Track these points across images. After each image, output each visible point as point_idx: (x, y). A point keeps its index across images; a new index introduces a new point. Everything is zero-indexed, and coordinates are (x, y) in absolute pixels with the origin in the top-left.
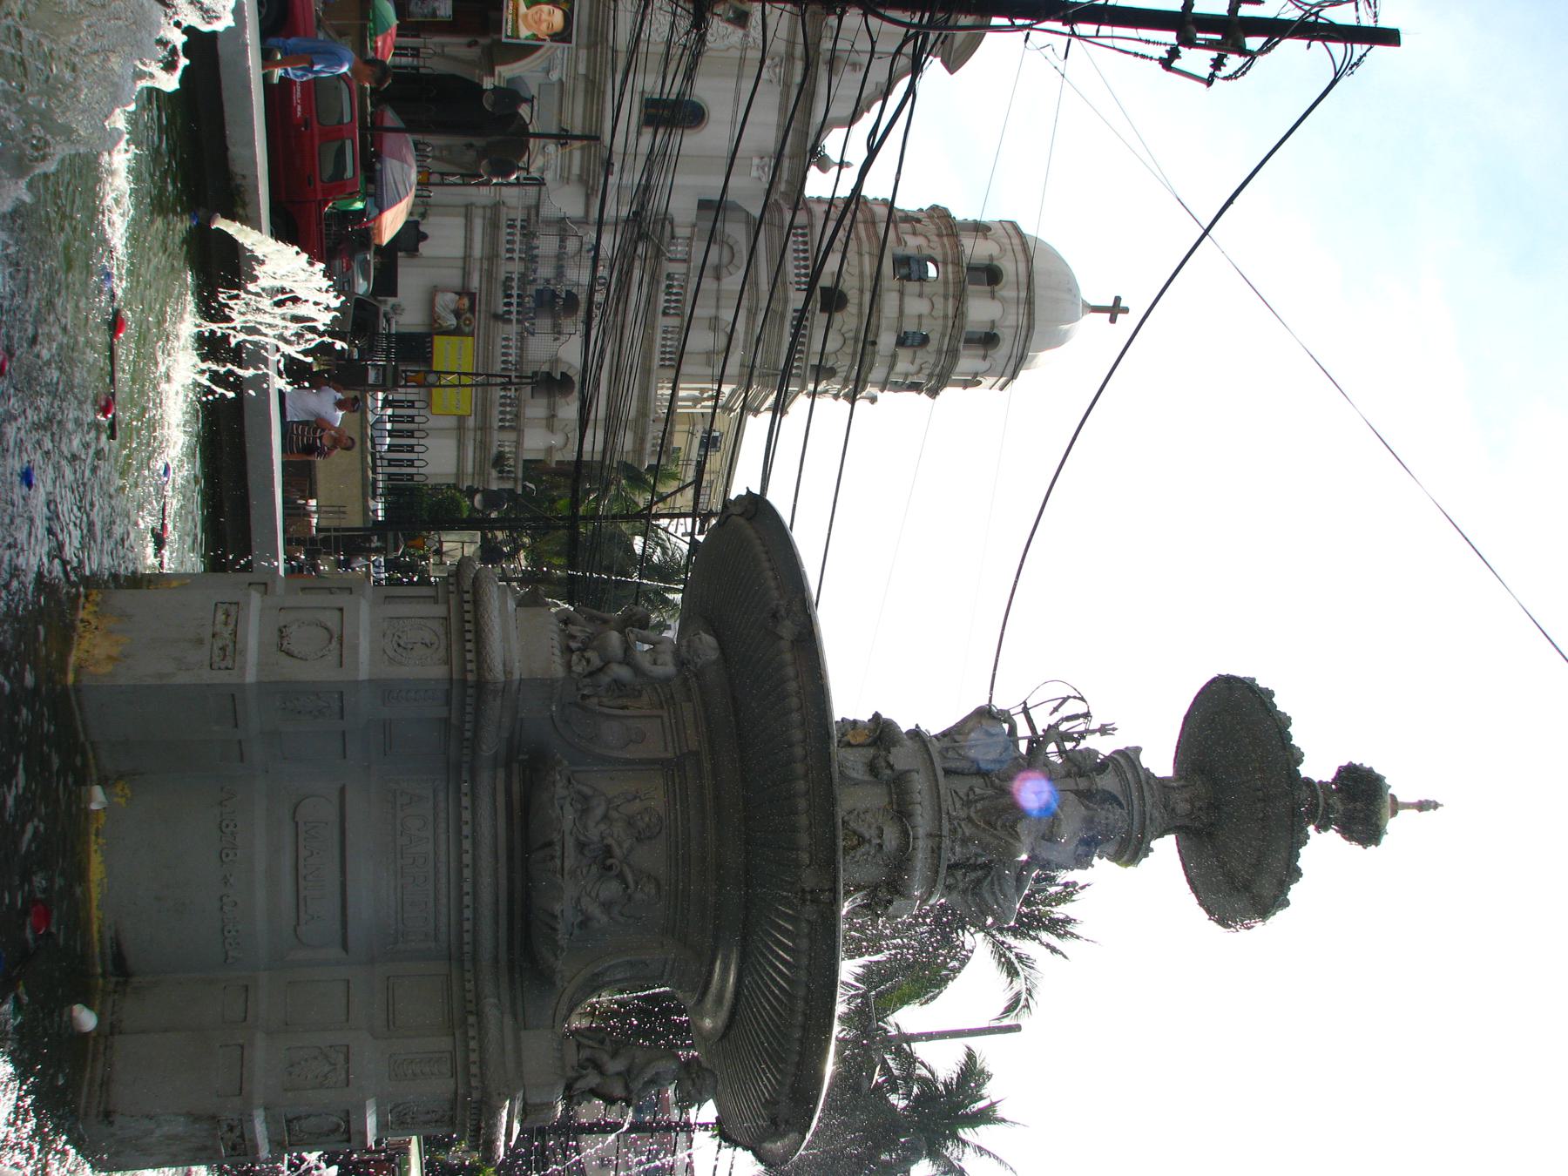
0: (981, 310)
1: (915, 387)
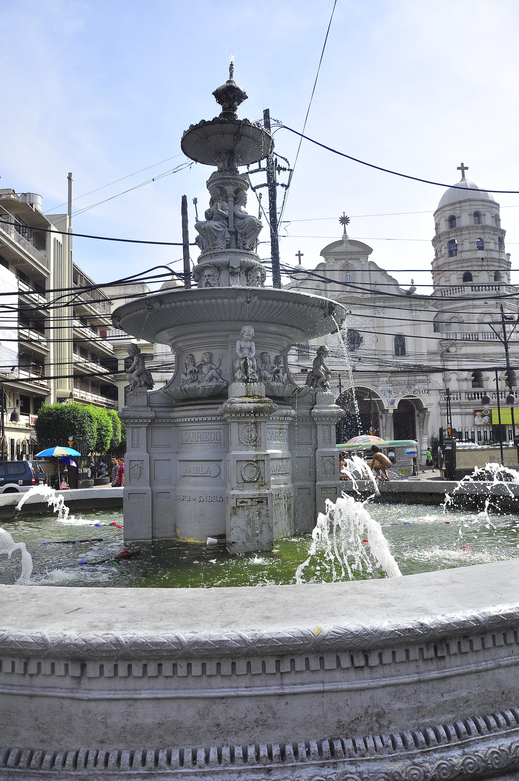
0: (465, 220)
1: (501, 241)
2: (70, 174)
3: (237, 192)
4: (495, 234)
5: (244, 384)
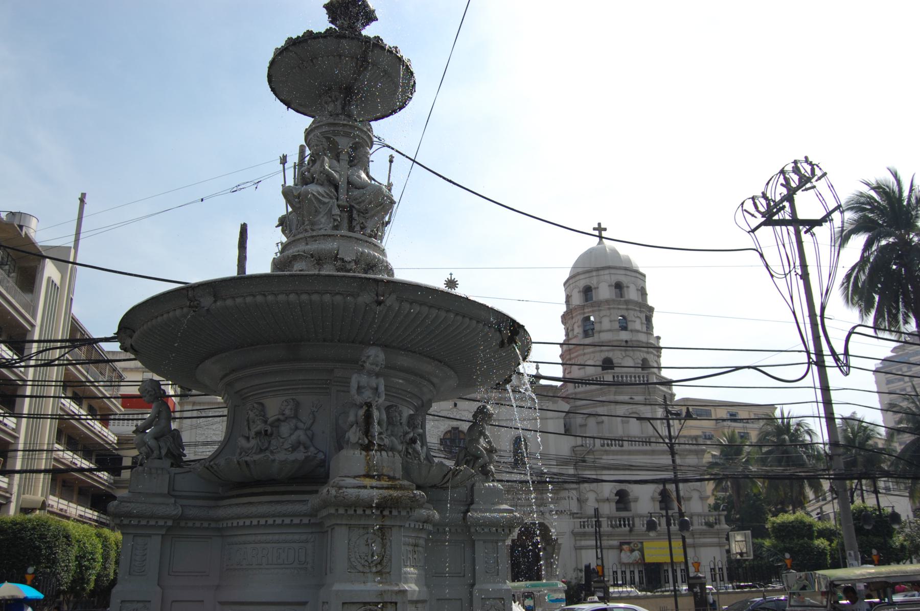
0: (604, 292)
1: (649, 320)
2: (84, 195)
3: (356, 147)
4: (641, 311)
5: (364, 453)
